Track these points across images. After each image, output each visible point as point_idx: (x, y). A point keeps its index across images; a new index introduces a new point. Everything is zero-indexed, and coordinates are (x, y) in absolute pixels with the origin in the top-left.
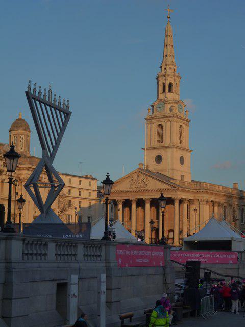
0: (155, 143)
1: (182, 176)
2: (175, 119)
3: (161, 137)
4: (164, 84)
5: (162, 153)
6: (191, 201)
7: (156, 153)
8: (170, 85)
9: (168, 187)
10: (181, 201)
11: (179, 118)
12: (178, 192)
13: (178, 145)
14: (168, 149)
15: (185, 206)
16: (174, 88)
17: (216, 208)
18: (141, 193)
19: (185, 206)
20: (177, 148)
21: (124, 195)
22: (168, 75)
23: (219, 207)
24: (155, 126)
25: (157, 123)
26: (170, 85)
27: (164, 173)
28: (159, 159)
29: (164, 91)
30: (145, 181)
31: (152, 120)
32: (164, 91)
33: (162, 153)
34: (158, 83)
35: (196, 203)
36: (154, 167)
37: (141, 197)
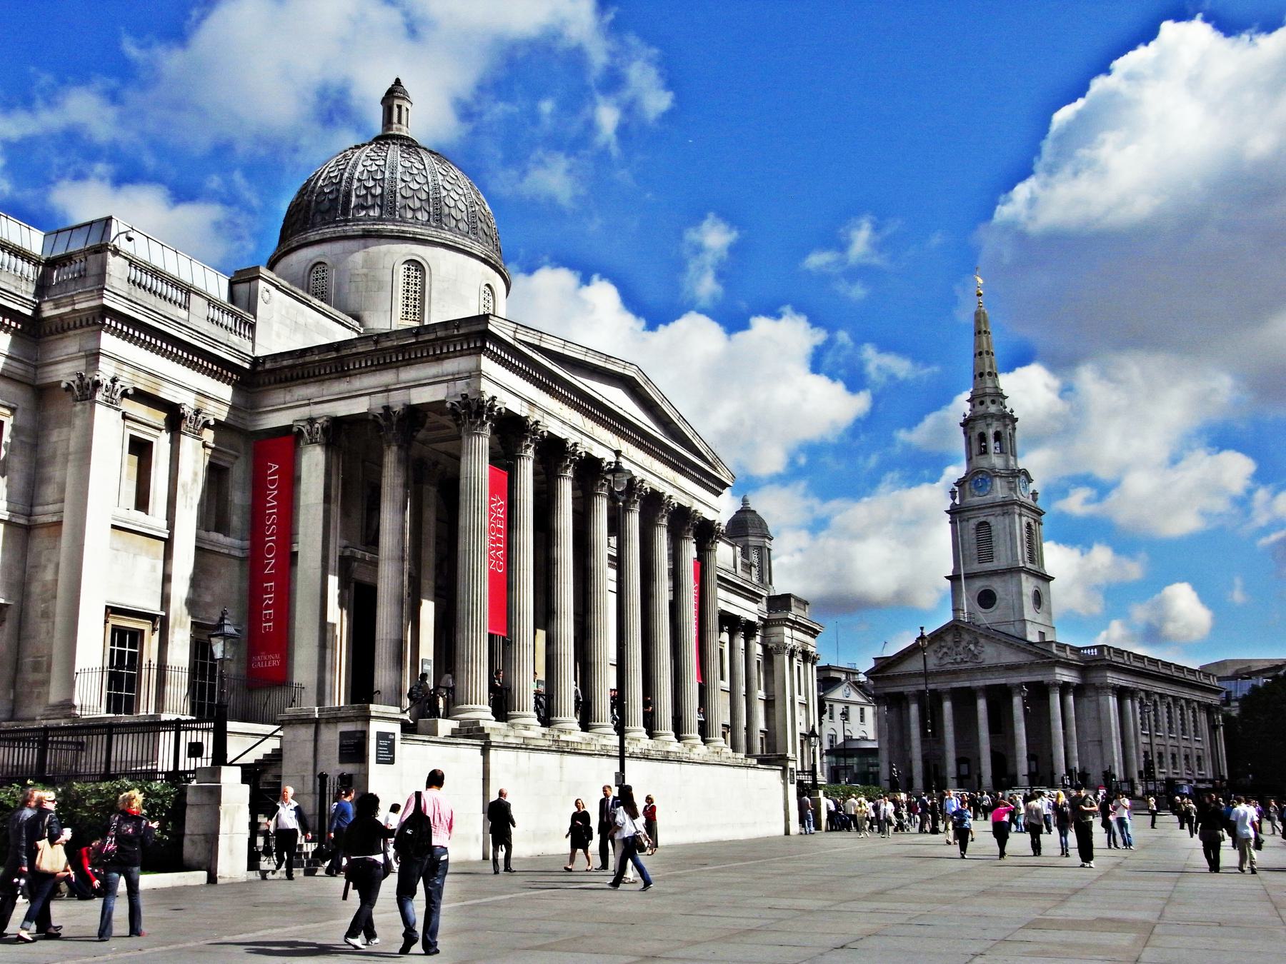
1: (1042, 634)
3: (986, 553)
5: (996, 585)
6: (1079, 691)
7: (979, 585)
9: (1032, 658)
10: (1065, 688)
12: (1058, 670)
13: (1029, 565)
14: (1007, 577)
15: (1071, 699)
18: (964, 676)
22: (992, 416)
25: (972, 523)
26: (998, 436)
27: (1002, 628)
28: (987, 599)
30: (972, 647)
32: (984, 451)
33: (996, 585)
36: (985, 617)
37: (967, 684)
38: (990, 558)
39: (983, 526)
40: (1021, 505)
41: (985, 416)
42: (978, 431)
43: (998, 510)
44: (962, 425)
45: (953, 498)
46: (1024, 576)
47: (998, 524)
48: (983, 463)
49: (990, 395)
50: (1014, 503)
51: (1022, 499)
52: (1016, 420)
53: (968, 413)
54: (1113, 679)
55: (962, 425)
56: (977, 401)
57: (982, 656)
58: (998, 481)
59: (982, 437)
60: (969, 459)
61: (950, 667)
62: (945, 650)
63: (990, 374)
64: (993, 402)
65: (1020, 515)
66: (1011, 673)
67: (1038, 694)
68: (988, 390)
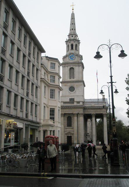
0: (69, 80)
5: (75, 85)
7: (69, 85)
8: (76, 45)
25: (69, 67)
26: (76, 45)
29: (72, 48)
32: (72, 48)
34: (66, 44)
38: (74, 78)
39: (72, 69)
41: (73, 40)
42: (71, 43)
43: (77, 65)
44: (66, 42)
48: (73, 51)
52: (80, 43)
53: (68, 39)
55: (66, 42)
56: (71, 36)
58: (76, 57)
60: (68, 50)
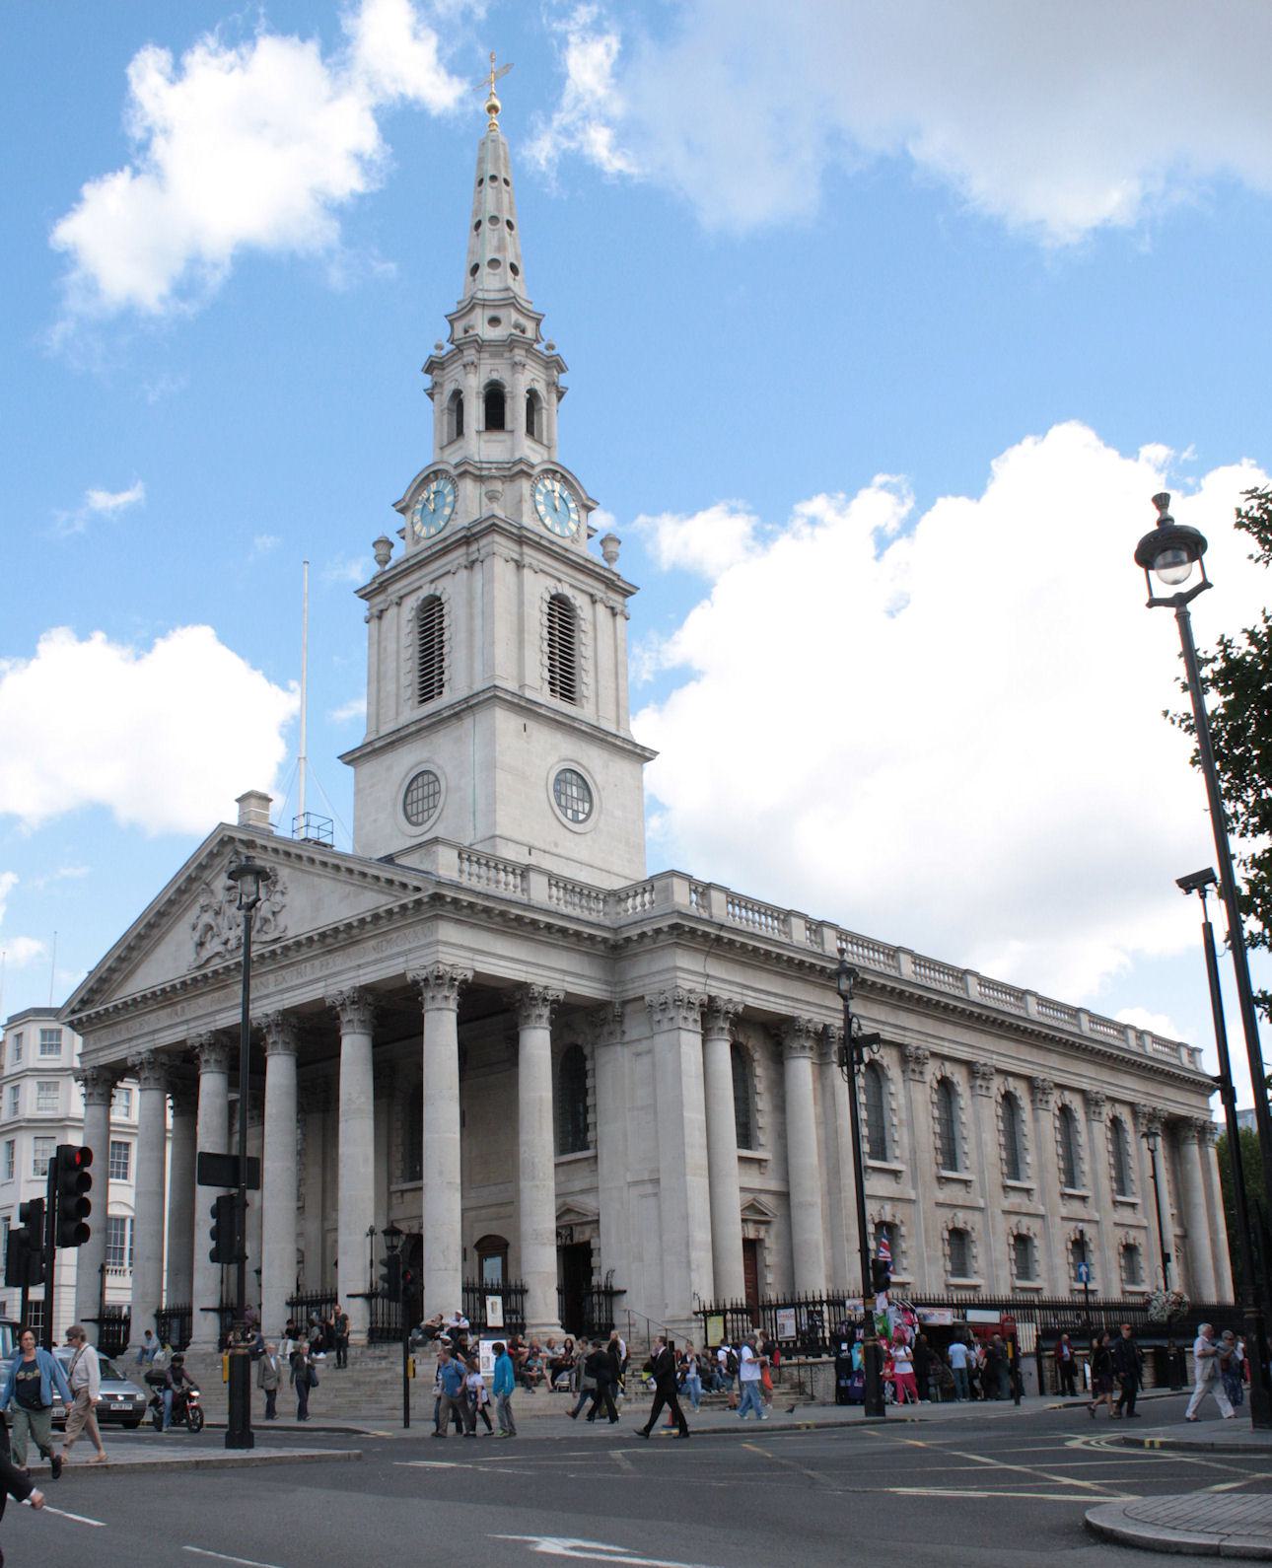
0: (412, 713)
2: (502, 546)
4: (457, 397)
5: (441, 752)
11: (538, 546)
12: (448, 932)
14: (468, 721)
15: (537, 1044)
16: (516, 411)
17: (802, 1069)
19: (537, 1044)
20: (524, 708)
21: (163, 1017)
22: (481, 345)
23: (822, 1064)
24: (403, 621)
25: (412, 603)
28: (420, 794)
31: (391, 589)
35: (634, 1028)
40: (521, 539)
43: (458, 556)
45: (383, 561)
46: (504, 722)
47: (452, 590)
48: (453, 456)
49: (484, 304)
50: (492, 527)
51: (527, 521)
54: (692, 974)
57: (282, 919)
59: (457, 399)
61: (217, 964)
62: (207, 918)
63: (494, 263)
64: (494, 321)
65: (519, 566)
66: (338, 962)
67: (394, 1015)
68: (480, 295)
